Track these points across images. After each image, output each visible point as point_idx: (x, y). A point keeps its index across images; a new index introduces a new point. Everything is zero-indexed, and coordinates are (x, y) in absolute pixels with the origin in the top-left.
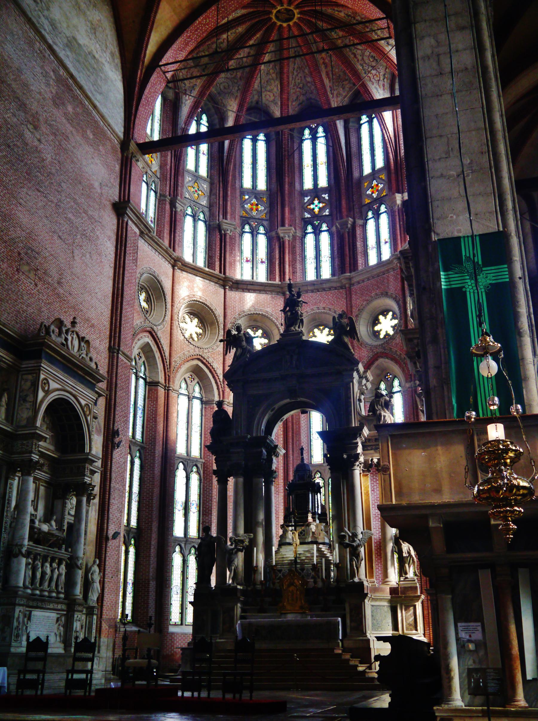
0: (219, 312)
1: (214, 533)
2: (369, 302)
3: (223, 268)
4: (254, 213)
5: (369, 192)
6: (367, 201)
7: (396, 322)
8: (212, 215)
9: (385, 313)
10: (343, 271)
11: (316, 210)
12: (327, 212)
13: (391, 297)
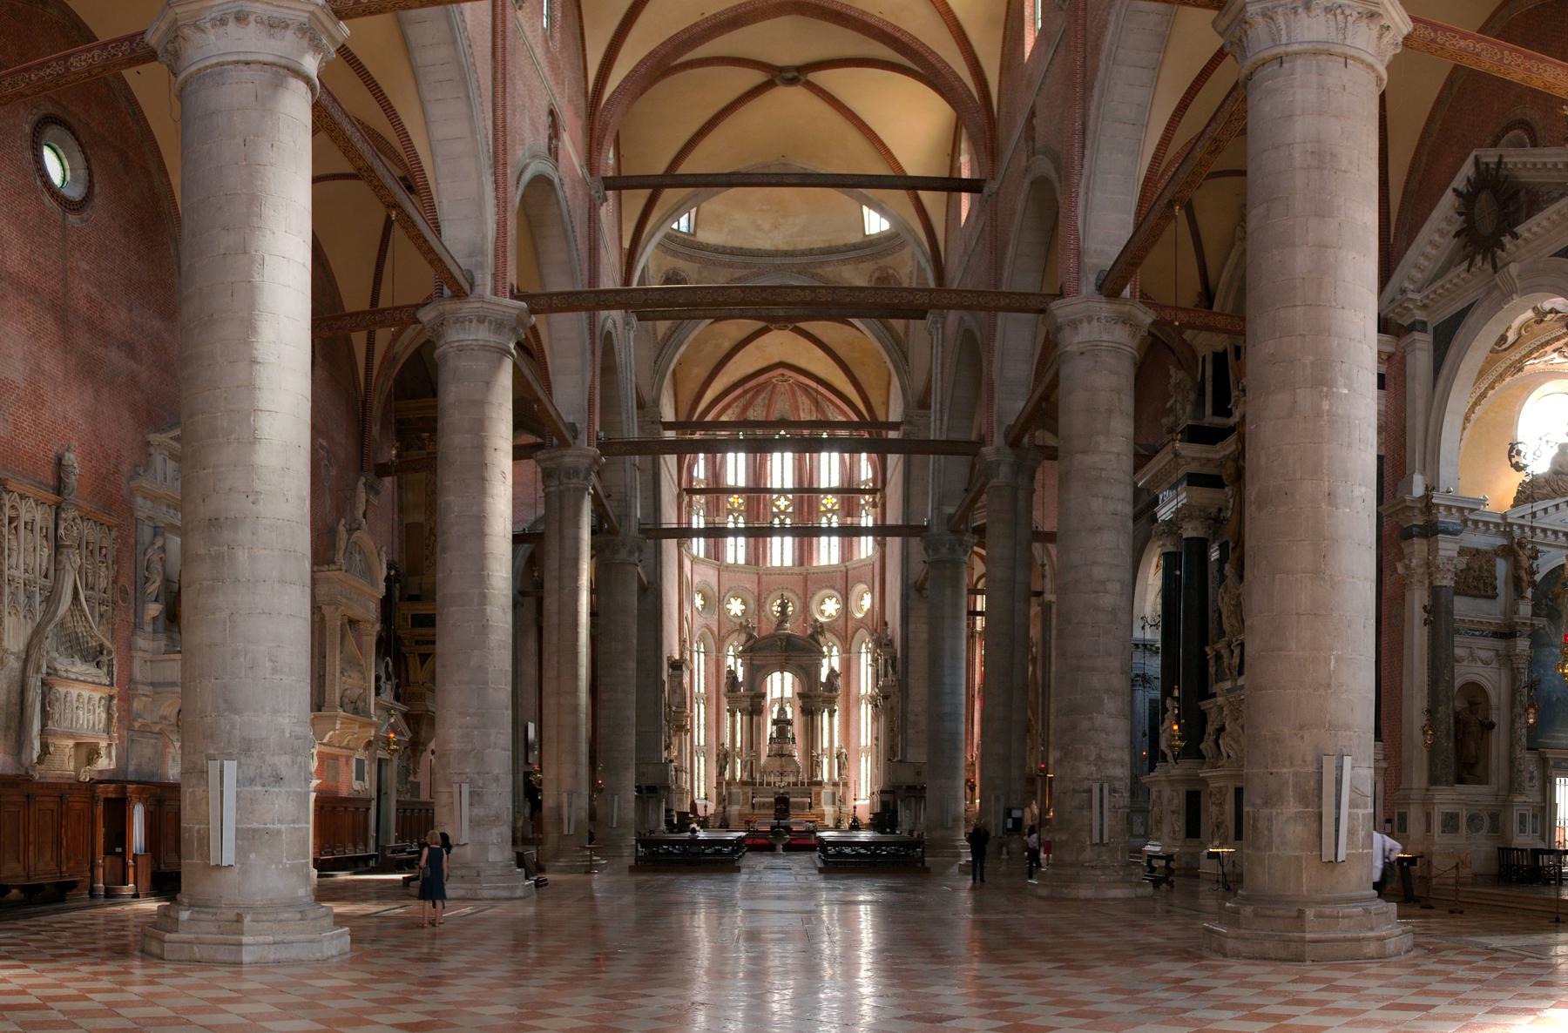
2: (820, 589)
4: (736, 505)
5: (824, 501)
6: (823, 509)
7: (838, 606)
9: (830, 597)
11: (782, 508)
12: (790, 510)
13: (837, 590)
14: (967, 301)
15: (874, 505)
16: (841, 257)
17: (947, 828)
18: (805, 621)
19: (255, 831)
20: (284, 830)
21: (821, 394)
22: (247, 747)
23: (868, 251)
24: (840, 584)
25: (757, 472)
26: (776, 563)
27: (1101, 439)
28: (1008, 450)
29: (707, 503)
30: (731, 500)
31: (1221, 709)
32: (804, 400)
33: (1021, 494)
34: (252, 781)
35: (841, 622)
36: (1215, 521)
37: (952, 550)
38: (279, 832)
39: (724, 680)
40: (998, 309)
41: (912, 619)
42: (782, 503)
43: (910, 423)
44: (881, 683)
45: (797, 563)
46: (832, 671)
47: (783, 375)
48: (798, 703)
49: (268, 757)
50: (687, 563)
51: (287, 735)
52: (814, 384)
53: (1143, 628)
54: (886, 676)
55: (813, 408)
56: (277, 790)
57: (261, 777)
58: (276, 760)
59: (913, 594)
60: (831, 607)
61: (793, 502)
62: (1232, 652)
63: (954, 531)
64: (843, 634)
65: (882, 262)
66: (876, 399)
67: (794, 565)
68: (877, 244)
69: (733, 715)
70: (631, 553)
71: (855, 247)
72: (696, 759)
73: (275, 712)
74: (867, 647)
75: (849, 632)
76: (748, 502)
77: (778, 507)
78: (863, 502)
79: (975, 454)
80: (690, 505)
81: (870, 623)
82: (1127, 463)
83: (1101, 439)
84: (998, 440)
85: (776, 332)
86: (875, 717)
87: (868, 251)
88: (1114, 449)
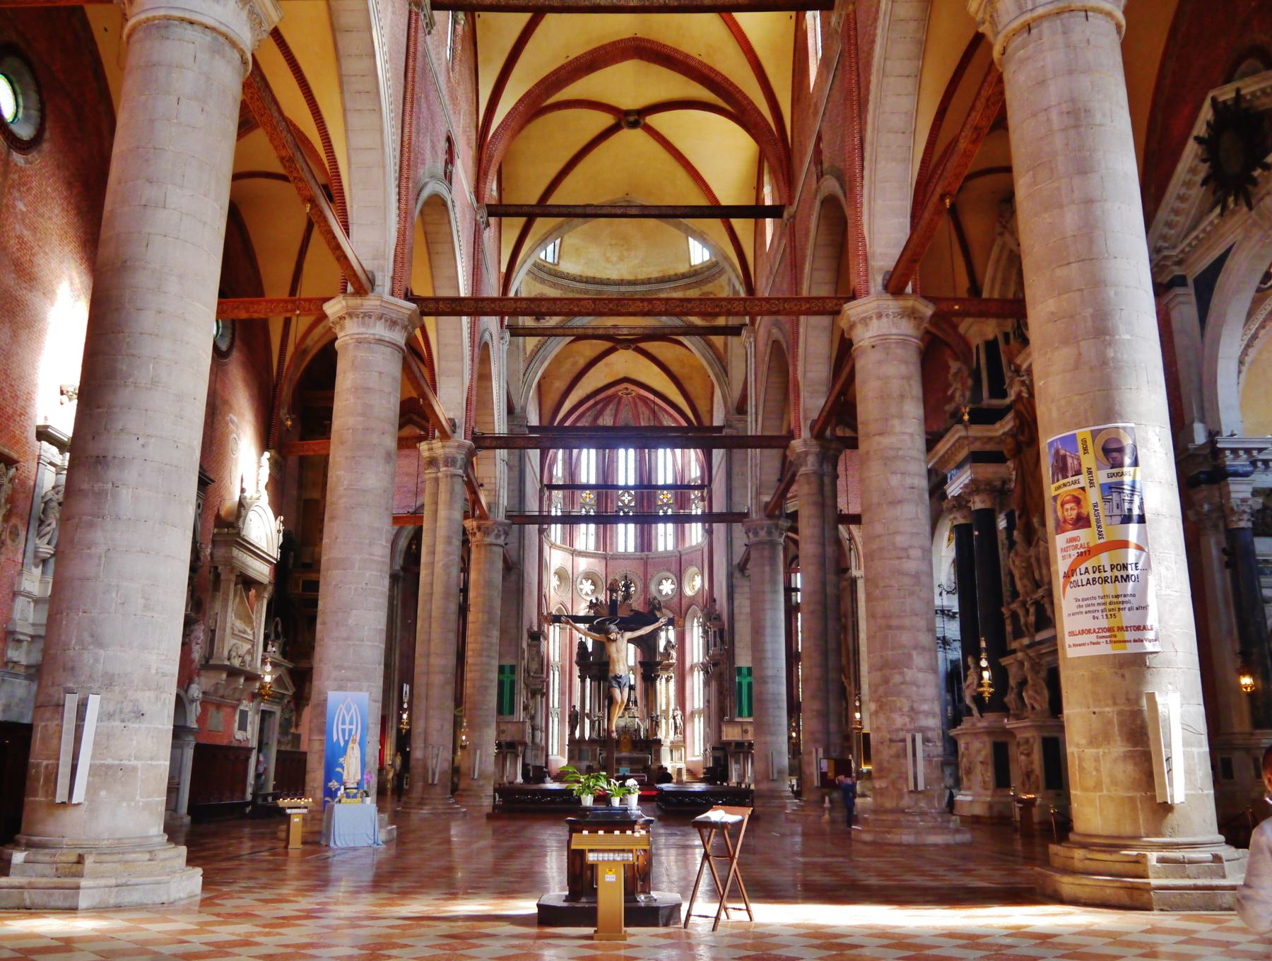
0: (570, 572)
1: (578, 708)
2: (658, 572)
3: (571, 544)
5: (661, 497)
6: (660, 503)
7: (673, 586)
8: (565, 504)
9: (667, 579)
10: (642, 551)
11: (626, 502)
12: (633, 504)
13: (672, 573)
14: (773, 307)
15: (703, 499)
16: (672, 285)
17: (773, 780)
18: (645, 599)
19: (109, 767)
20: (140, 766)
21: (658, 405)
22: (109, 682)
23: (693, 280)
24: (674, 567)
25: (606, 469)
26: (621, 549)
27: (896, 422)
28: (814, 442)
29: (564, 498)
30: (584, 495)
31: (1021, 664)
32: (642, 409)
33: (827, 480)
34: (110, 716)
35: (676, 600)
36: (999, 492)
37: (770, 533)
38: (134, 769)
39: (575, 650)
40: (801, 313)
41: (736, 596)
42: (626, 498)
43: (730, 427)
44: (711, 652)
45: (639, 549)
46: (669, 642)
47: (627, 389)
48: (640, 670)
49: (130, 693)
50: (546, 548)
51: (153, 671)
52: (651, 397)
53: (941, 594)
54: (715, 646)
55: (652, 418)
56: (137, 725)
57: (121, 712)
58: (139, 695)
59: (737, 574)
60: (667, 587)
61: (635, 497)
62: (1027, 611)
63: (770, 516)
64: (678, 610)
65: (708, 288)
66: (702, 406)
67: (636, 551)
68: (702, 273)
69: (583, 681)
70: (498, 536)
71: (684, 276)
72: (551, 719)
73: (144, 648)
74: (698, 622)
75: (683, 609)
76: (599, 497)
77: (623, 501)
78: (693, 497)
79: (786, 447)
80: (550, 498)
81: (701, 601)
82: (920, 443)
83: (896, 422)
84: (805, 433)
85: (621, 351)
86: (707, 684)
87: (693, 280)
88: (908, 431)
